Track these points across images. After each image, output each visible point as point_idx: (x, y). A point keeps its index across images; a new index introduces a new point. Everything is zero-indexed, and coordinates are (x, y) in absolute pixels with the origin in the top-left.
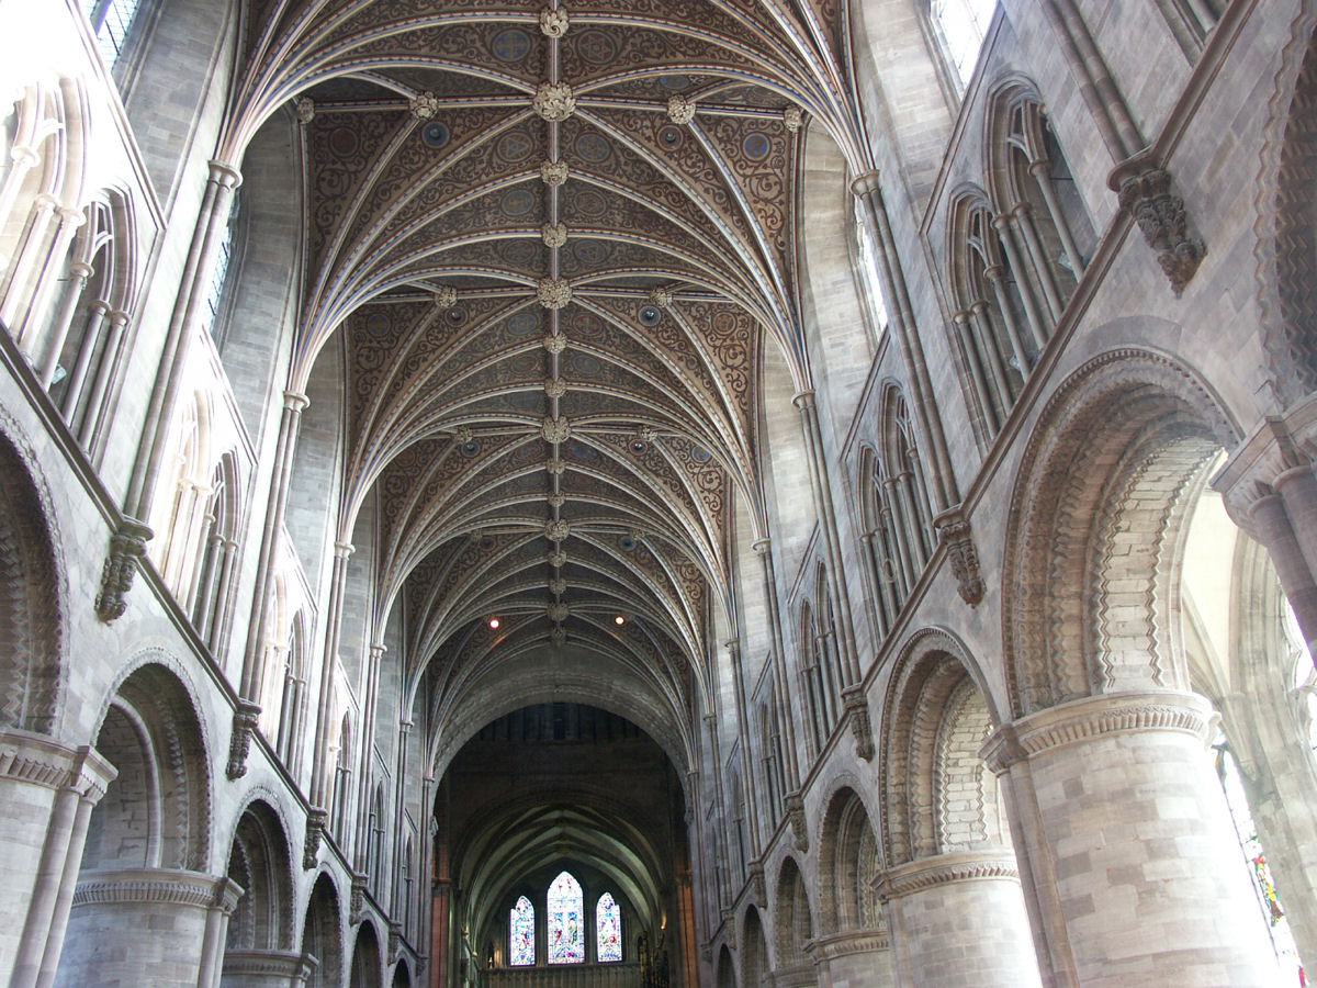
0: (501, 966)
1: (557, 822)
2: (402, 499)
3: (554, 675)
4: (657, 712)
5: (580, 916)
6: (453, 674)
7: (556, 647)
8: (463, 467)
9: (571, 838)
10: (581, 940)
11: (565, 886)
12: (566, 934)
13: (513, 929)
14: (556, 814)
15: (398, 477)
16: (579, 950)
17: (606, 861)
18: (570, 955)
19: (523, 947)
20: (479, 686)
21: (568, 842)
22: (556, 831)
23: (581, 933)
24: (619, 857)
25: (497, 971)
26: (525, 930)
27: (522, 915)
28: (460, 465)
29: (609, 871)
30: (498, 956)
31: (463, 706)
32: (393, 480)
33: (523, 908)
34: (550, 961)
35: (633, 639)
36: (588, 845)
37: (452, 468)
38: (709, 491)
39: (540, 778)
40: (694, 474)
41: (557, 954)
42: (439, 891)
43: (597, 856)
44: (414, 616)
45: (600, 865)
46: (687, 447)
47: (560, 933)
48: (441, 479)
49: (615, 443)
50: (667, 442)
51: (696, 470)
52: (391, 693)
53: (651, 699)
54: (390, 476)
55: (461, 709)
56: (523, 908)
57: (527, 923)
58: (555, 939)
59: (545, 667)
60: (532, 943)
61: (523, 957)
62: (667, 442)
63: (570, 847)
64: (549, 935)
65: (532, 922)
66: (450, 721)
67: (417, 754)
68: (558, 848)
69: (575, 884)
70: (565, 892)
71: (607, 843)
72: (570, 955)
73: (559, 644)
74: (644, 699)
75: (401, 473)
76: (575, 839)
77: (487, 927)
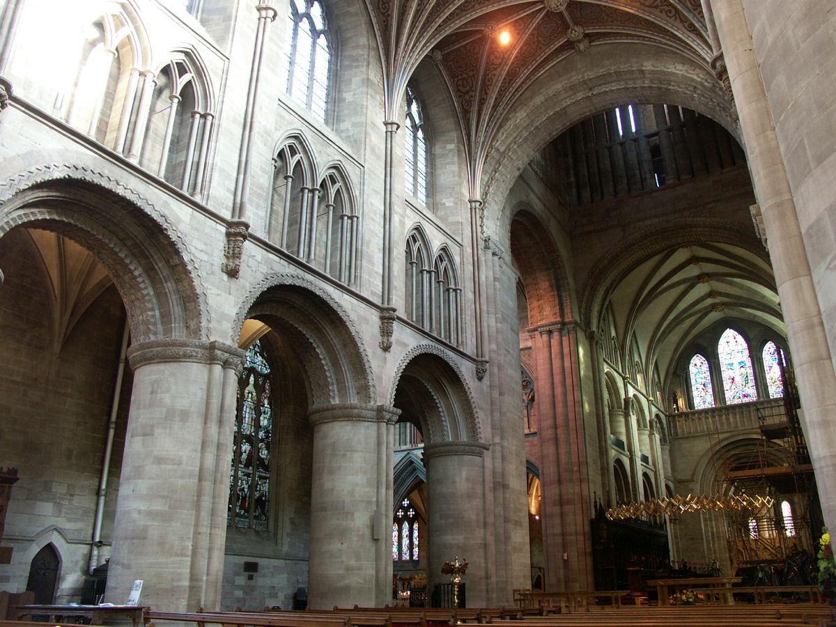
0: (685, 410)
1: (701, 278)
3: (583, 77)
4: (695, 77)
5: (749, 363)
6: (482, 102)
7: (580, 51)
9: (720, 294)
10: (752, 383)
11: (732, 341)
12: (738, 379)
13: (693, 381)
14: (693, 271)
16: (751, 391)
17: (758, 309)
18: (745, 396)
19: (703, 394)
20: (513, 109)
21: (718, 300)
22: (701, 289)
23: (751, 377)
24: (764, 301)
25: (681, 415)
26: (703, 381)
27: (698, 368)
29: (763, 320)
30: (681, 402)
31: (502, 130)
33: (699, 364)
34: (728, 403)
35: (649, 6)
36: (739, 298)
39: (649, 222)
41: (733, 395)
42: (566, 330)
43: (747, 306)
44: (386, 26)
45: (755, 316)
47: (733, 379)
52: (362, 93)
53: (686, 67)
55: (500, 134)
56: (699, 364)
57: (704, 375)
58: (730, 385)
59: (574, 73)
60: (710, 390)
61: (704, 402)
63: (723, 304)
64: (724, 383)
65: (708, 373)
66: (491, 146)
67: (457, 179)
68: (713, 307)
69: (740, 338)
70: (732, 346)
71: (749, 289)
72: (745, 396)
73: (582, 47)
74: (679, 69)
76: (727, 295)
77: (669, 381)
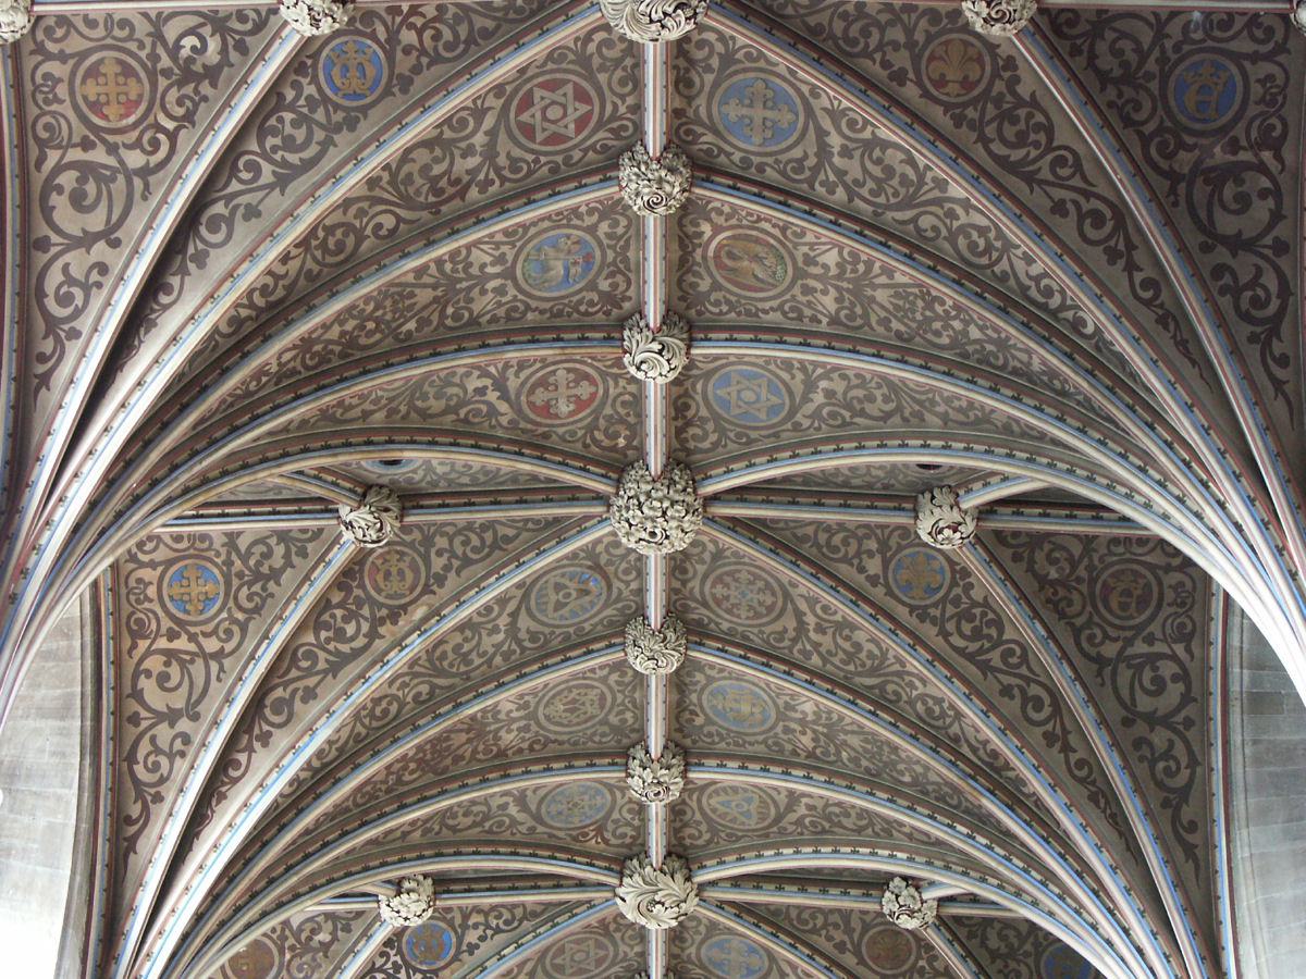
2: (184, 725)
8: (373, 635)
15: (170, 655)
28: (365, 627)
32: (155, 664)
37: (340, 635)
38: (1152, 720)
40: (1100, 661)
46: (1082, 572)
48: (309, 672)
49: (846, 560)
50: (1016, 558)
51: (1109, 650)
54: (148, 653)
62: (1016, 558)
75: (182, 644)
